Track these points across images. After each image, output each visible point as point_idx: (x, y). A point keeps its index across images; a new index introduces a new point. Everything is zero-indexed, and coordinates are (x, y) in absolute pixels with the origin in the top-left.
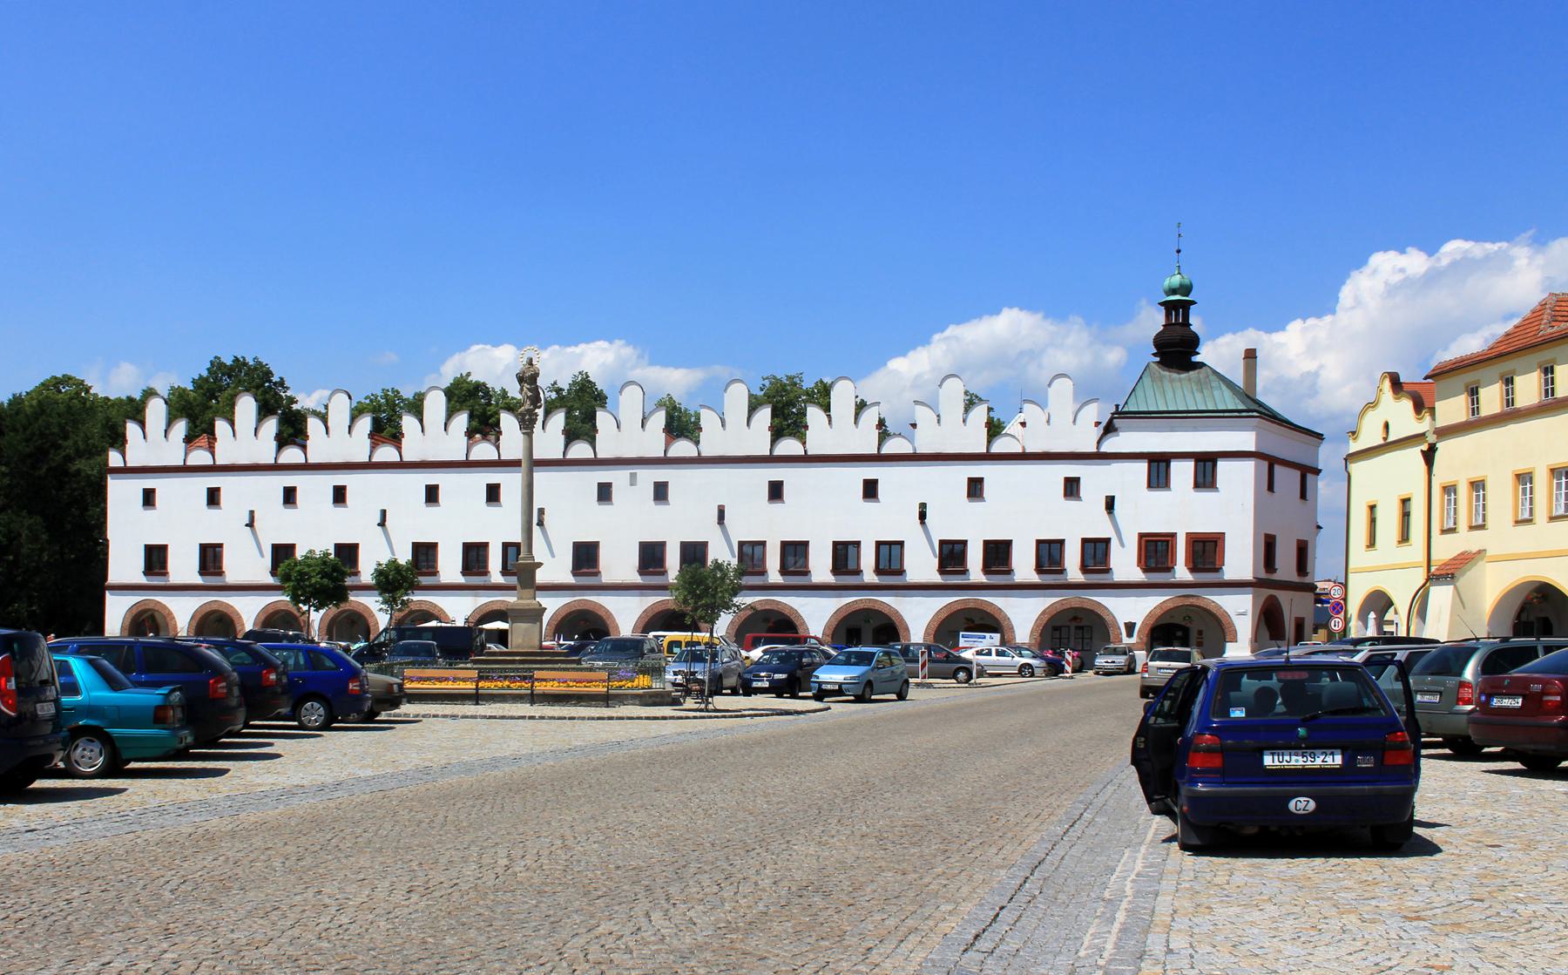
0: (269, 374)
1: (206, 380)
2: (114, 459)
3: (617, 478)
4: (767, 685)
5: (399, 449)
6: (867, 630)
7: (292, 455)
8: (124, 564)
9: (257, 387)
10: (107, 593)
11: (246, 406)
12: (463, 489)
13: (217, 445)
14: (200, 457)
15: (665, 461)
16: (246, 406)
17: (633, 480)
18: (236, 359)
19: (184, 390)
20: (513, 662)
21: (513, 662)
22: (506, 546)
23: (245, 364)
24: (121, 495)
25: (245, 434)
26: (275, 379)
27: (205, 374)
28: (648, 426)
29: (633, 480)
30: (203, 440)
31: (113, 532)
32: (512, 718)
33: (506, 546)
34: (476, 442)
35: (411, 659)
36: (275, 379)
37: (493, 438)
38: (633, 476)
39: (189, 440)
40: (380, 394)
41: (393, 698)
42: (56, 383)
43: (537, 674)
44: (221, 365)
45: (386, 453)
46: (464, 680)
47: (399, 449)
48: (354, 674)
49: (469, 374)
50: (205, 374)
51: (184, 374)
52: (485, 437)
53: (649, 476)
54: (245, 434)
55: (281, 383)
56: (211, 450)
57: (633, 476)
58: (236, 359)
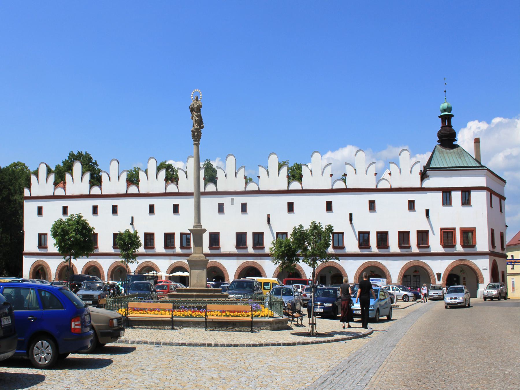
0: (91, 159)
1: (68, 161)
2: (27, 193)
3: (226, 200)
4: (322, 310)
5: (138, 187)
6: (460, 278)
7: (96, 191)
8: (30, 244)
9: (86, 165)
10: (24, 257)
11: (77, 167)
12: (164, 206)
13: (67, 186)
14: (60, 192)
15: (245, 193)
16: (77, 167)
17: (232, 203)
18: (79, 153)
19: (59, 165)
20: (192, 296)
21: (192, 296)
22: (182, 234)
23: (82, 155)
24: (29, 209)
25: (78, 182)
26: (93, 161)
27: (67, 159)
28: (238, 176)
29: (232, 203)
30: (62, 184)
31: (26, 228)
32: (196, 345)
33: (182, 234)
34: (169, 184)
35: (137, 292)
36: (93, 161)
37: (175, 183)
38: (232, 200)
39: (56, 184)
40: (133, 169)
41: (114, 330)
42: (15, 165)
43: (209, 307)
44: (73, 155)
45: (133, 189)
46: (165, 310)
47: (138, 187)
48: (78, 312)
49: (166, 162)
50: (67, 159)
51: (58, 160)
52: (172, 182)
53: (240, 200)
54: (78, 182)
55: (95, 163)
56: (64, 188)
57: (232, 200)
58: (79, 153)
